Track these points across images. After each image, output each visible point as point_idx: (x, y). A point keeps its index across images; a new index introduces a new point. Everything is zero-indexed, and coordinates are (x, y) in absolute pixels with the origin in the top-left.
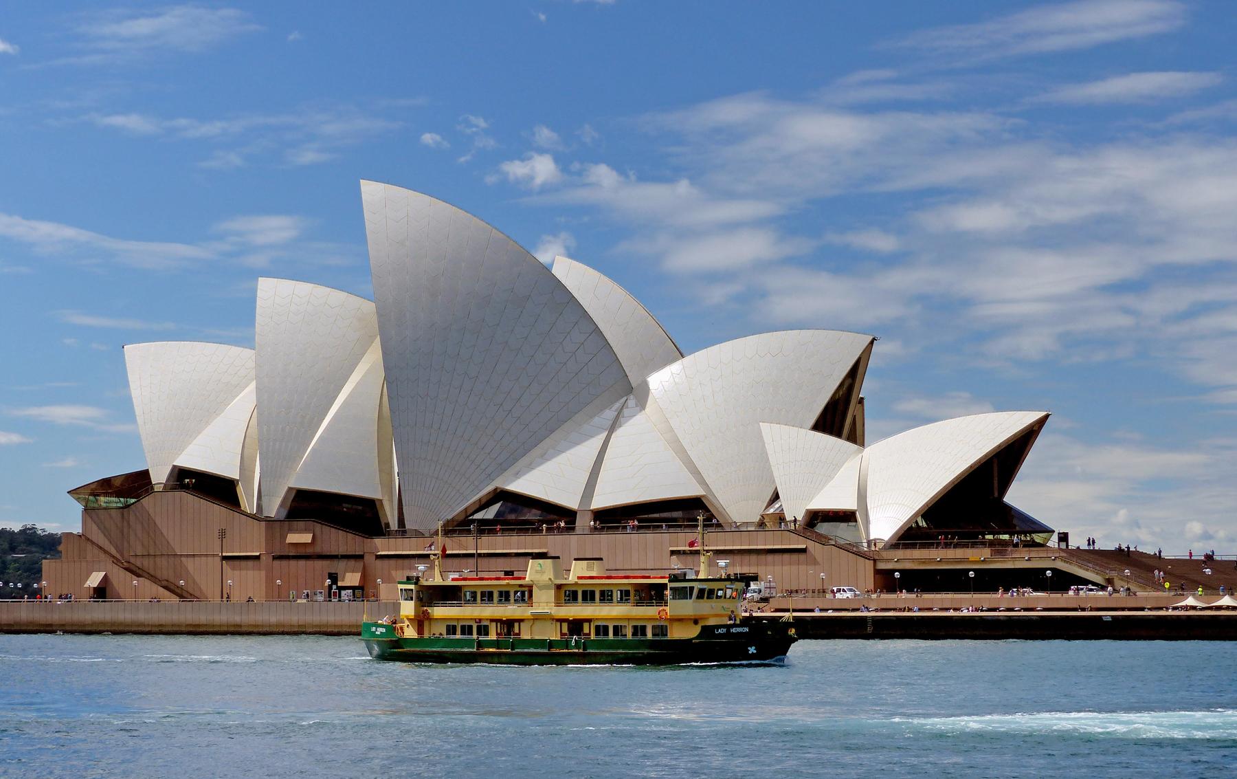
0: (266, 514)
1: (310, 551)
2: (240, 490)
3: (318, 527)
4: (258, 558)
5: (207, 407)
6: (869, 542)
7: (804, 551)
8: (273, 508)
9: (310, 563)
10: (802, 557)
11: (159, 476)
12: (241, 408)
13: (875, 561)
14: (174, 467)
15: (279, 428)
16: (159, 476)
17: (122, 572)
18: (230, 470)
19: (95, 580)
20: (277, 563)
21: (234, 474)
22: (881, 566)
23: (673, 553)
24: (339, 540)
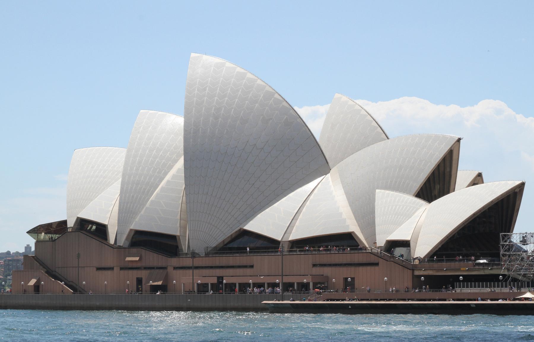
4: (112, 269)
10: (377, 268)
11: (71, 224)
14: (78, 218)
16: (71, 224)
19: (33, 282)
20: (122, 272)
22: (417, 273)
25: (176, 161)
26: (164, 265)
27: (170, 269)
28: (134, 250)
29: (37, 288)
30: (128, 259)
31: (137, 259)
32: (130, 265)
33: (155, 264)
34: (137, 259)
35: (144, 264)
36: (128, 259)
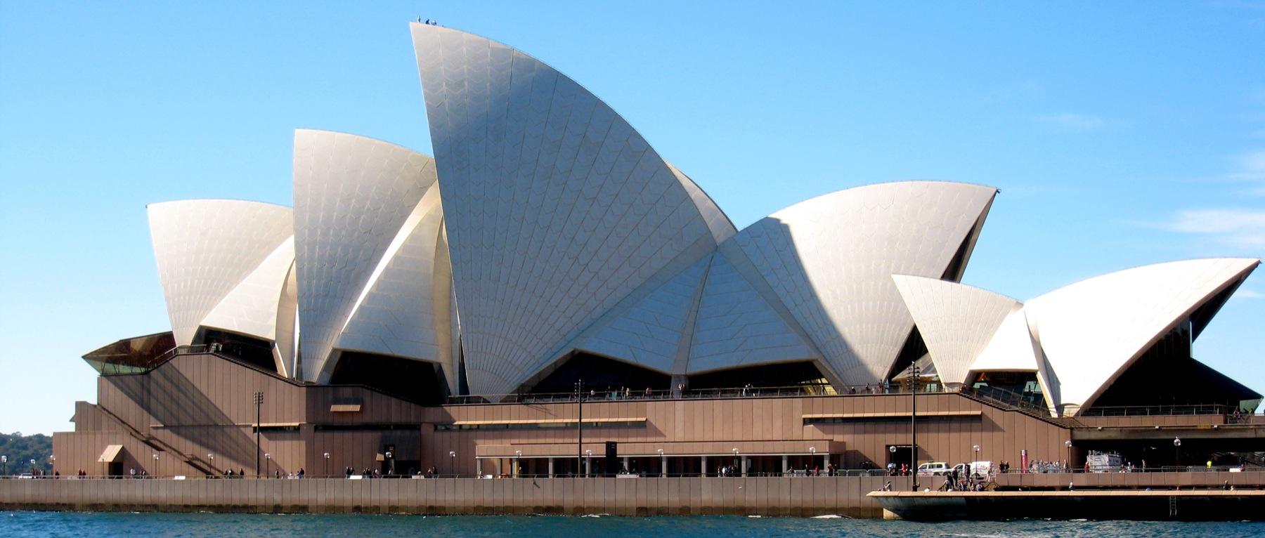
0: (305, 379)
1: (358, 420)
2: (277, 351)
3: (366, 394)
4: (297, 429)
5: (240, 263)
6: (1060, 408)
7: (978, 418)
8: (317, 371)
9: (358, 435)
11: (184, 338)
12: (280, 263)
13: (1072, 429)
14: (201, 328)
15: (321, 289)
16: (184, 338)
17: (142, 446)
18: (266, 331)
19: (110, 453)
20: (319, 435)
21: (270, 335)
23: (806, 422)
24: (393, 409)
25: (268, 246)
26: (413, 420)
27: (427, 430)
28: (347, 391)
29: (117, 468)
30: (334, 408)
31: (357, 408)
32: (338, 421)
33: (395, 418)
34: (357, 408)
35: (367, 419)
36: (334, 408)
